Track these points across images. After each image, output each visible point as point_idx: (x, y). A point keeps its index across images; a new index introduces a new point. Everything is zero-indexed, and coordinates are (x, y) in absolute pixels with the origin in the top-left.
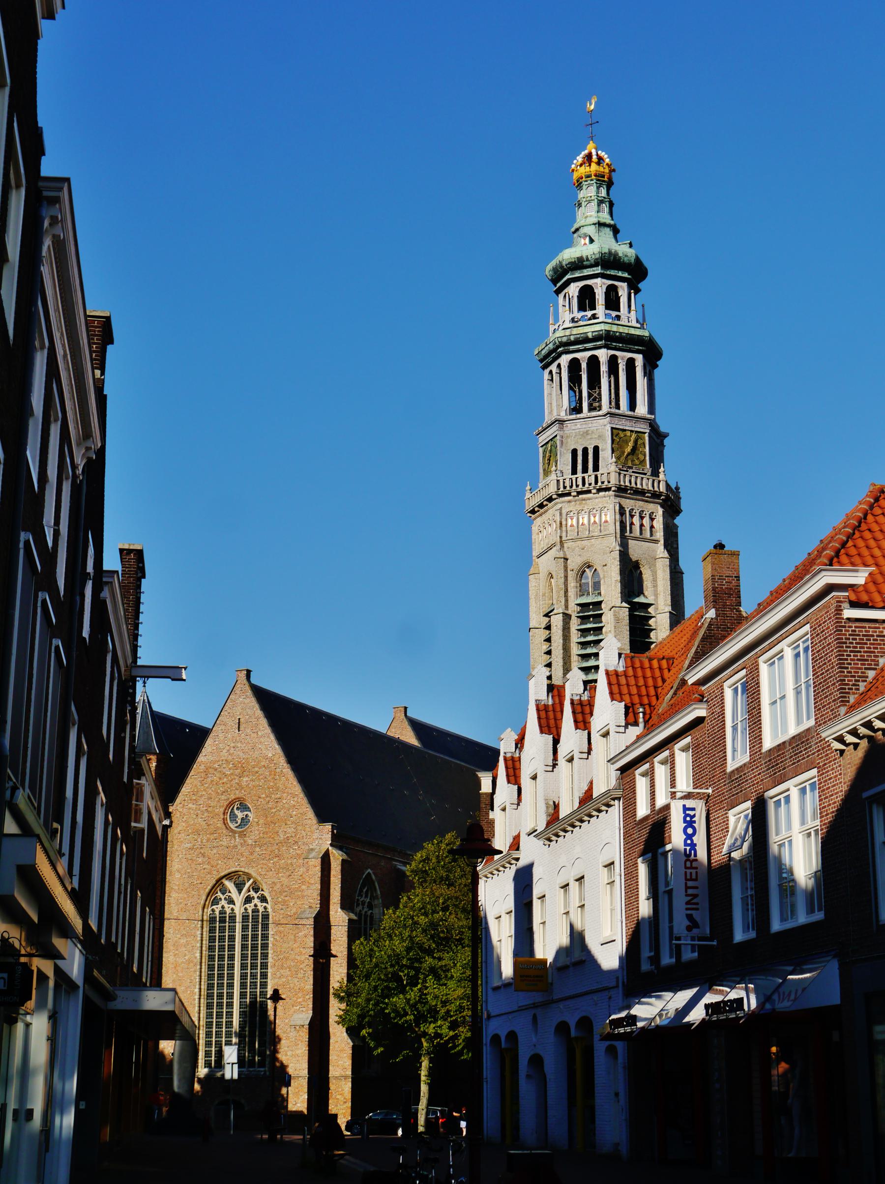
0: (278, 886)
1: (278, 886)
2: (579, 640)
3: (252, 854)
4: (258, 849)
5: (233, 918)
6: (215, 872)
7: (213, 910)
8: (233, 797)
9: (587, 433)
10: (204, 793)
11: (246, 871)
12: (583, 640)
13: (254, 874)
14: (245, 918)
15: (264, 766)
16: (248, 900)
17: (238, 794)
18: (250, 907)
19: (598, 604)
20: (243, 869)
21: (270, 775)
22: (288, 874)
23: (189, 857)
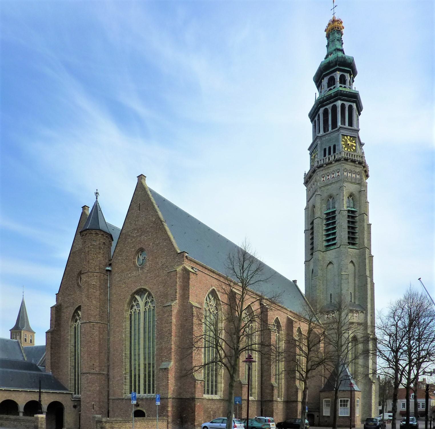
0: (159, 293)
1: (159, 293)
2: (325, 229)
3: (146, 278)
4: (149, 274)
5: (139, 313)
6: (130, 291)
7: (131, 312)
8: (137, 248)
9: (330, 140)
10: (125, 250)
11: (144, 287)
12: (327, 228)
13: (147, 289)
14: (145, 312)
15: (151, 227)
16: (146, 303)
17: (140, 246)
18: (147, 307)
19: (334, 212)
20: (142, 287)
21: (154, 231)
22: (163, 285)
23: (119, 285)
